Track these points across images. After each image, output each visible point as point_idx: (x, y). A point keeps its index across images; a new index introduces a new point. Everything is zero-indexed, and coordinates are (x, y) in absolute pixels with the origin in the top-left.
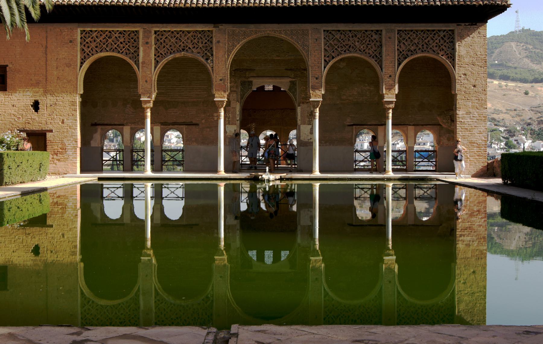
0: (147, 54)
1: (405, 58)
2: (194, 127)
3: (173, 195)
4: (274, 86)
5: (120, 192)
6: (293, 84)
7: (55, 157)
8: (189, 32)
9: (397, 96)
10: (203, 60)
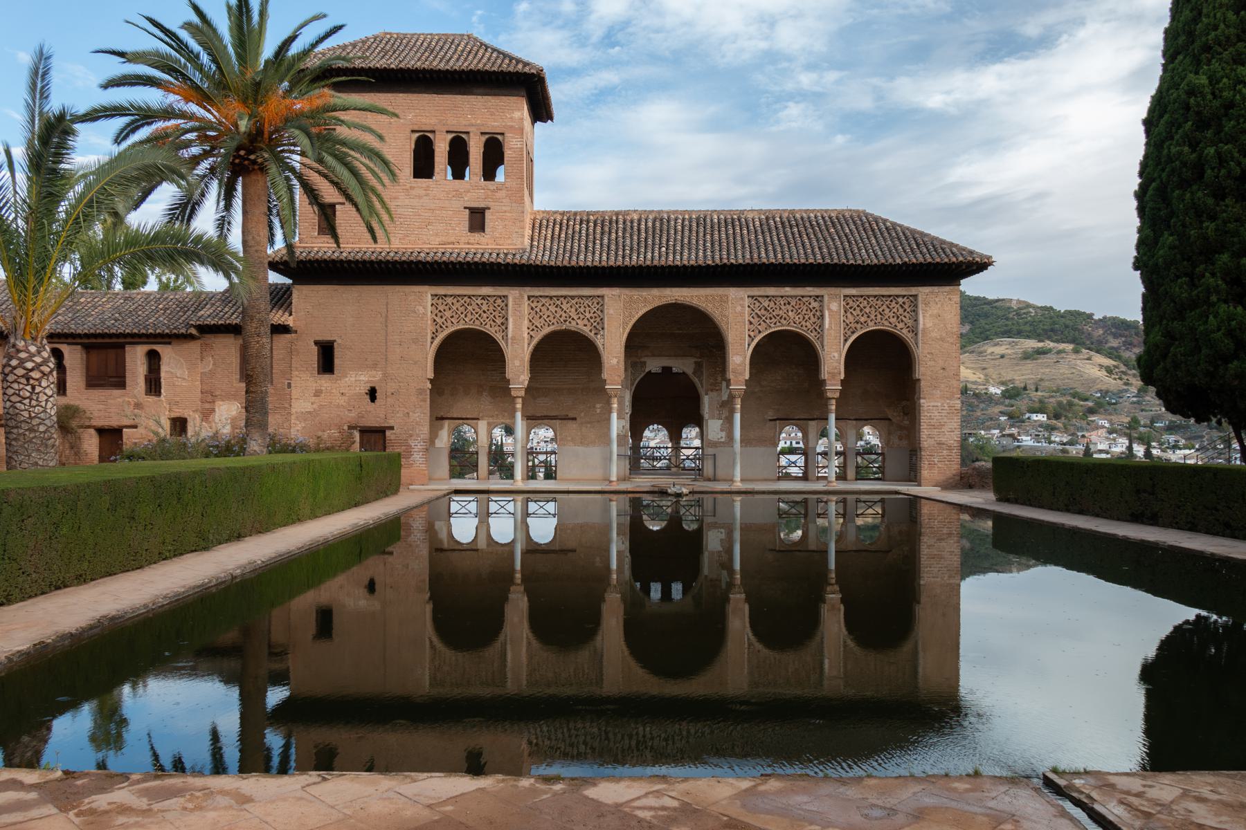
0: (518, 327)
3: (542, 511)
5: (473, 507)
6: (698, 366)
8: (573, 297)
10: (592, 334)
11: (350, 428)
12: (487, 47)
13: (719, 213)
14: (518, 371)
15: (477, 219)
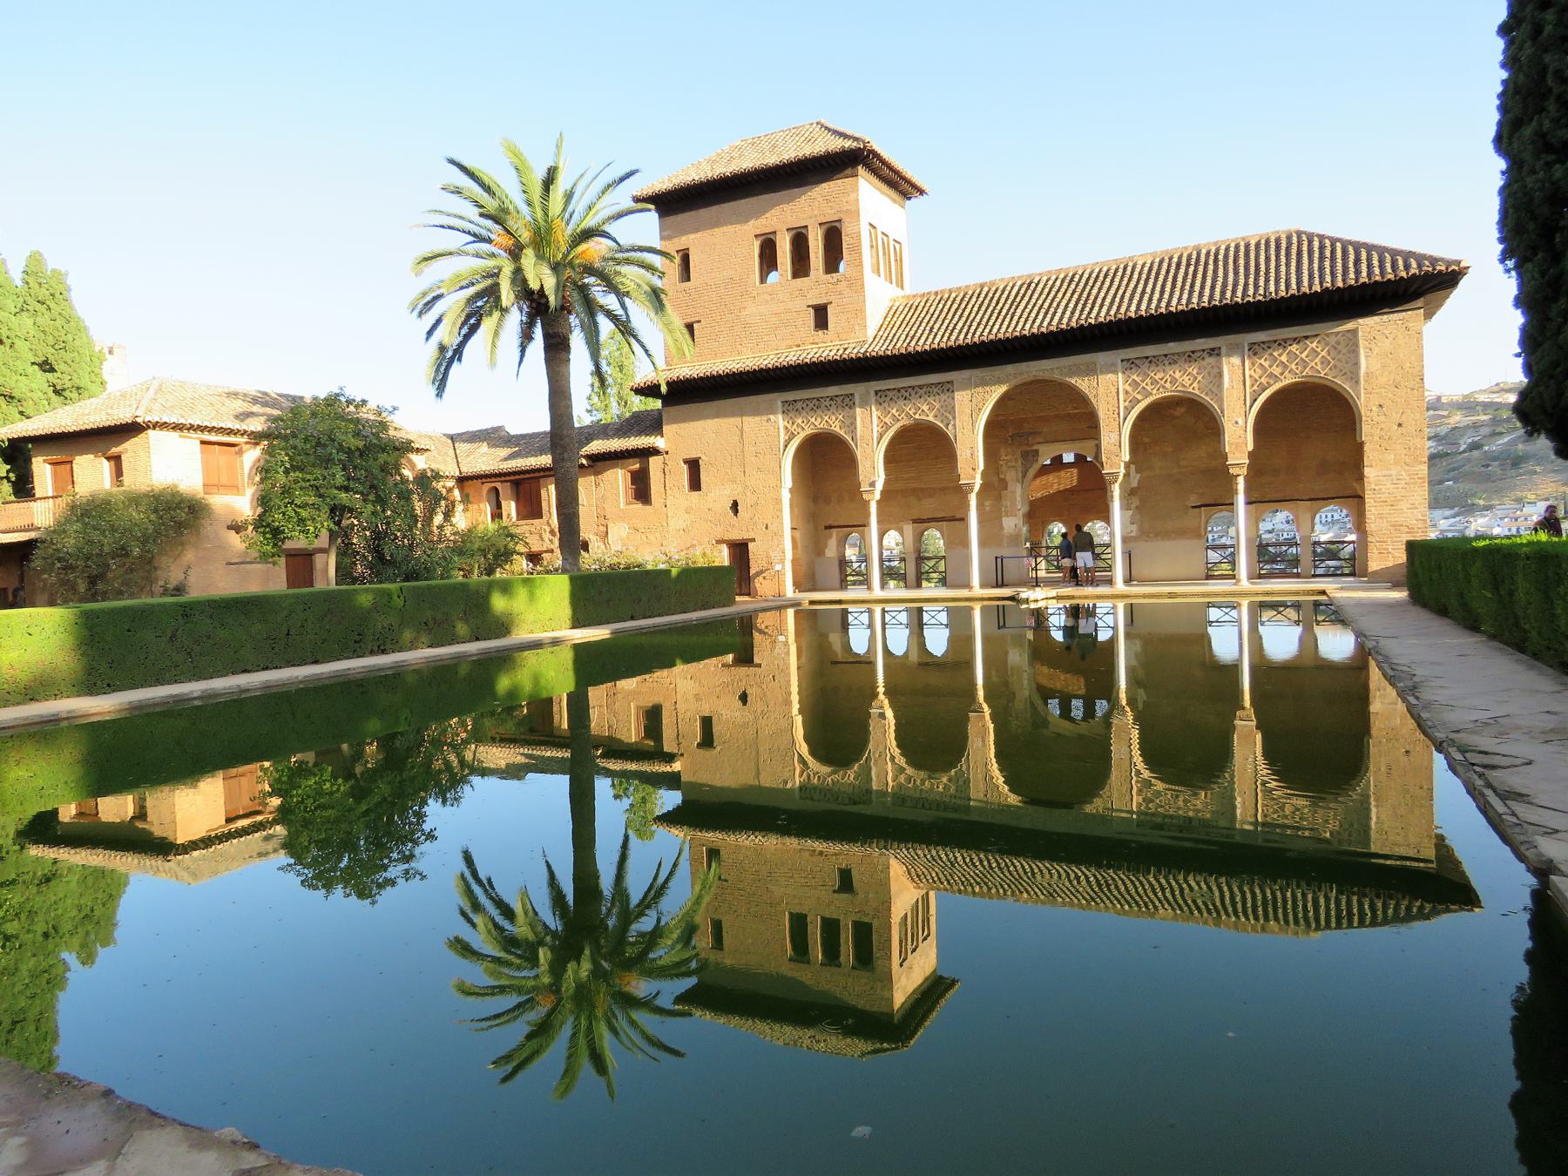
4: (1076, 455)
8: (921, 387)
15: (821, 316)
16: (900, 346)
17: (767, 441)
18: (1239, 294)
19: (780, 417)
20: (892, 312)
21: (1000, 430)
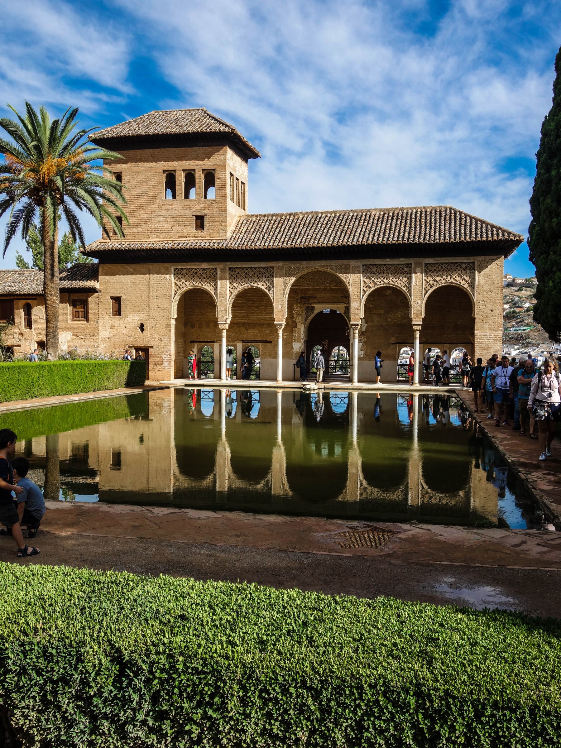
1: (431, 287)
2: (268, 344)
5: (211, 395)
7: (155, 367)
8: (255, 268)
9: (423, 320)
10: (267, 291)
11: (130, 347)
12: (210, 116)
13: (354, 211)
14: (225, 315)
15: (200, 222)
16: (247, 245)
17: (164, 291)
18: (422, 238)
19: (172, 276)
20: (240, 224)
21: (297, 296)
